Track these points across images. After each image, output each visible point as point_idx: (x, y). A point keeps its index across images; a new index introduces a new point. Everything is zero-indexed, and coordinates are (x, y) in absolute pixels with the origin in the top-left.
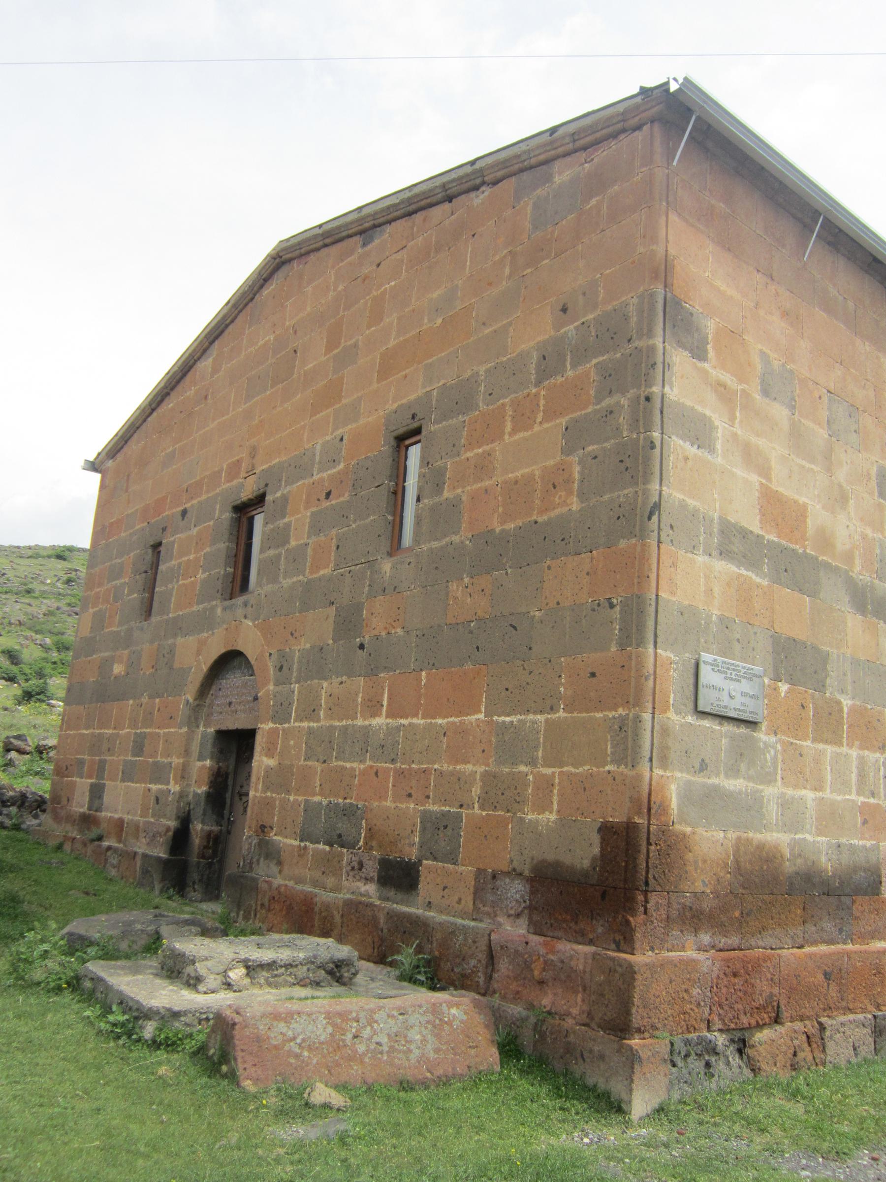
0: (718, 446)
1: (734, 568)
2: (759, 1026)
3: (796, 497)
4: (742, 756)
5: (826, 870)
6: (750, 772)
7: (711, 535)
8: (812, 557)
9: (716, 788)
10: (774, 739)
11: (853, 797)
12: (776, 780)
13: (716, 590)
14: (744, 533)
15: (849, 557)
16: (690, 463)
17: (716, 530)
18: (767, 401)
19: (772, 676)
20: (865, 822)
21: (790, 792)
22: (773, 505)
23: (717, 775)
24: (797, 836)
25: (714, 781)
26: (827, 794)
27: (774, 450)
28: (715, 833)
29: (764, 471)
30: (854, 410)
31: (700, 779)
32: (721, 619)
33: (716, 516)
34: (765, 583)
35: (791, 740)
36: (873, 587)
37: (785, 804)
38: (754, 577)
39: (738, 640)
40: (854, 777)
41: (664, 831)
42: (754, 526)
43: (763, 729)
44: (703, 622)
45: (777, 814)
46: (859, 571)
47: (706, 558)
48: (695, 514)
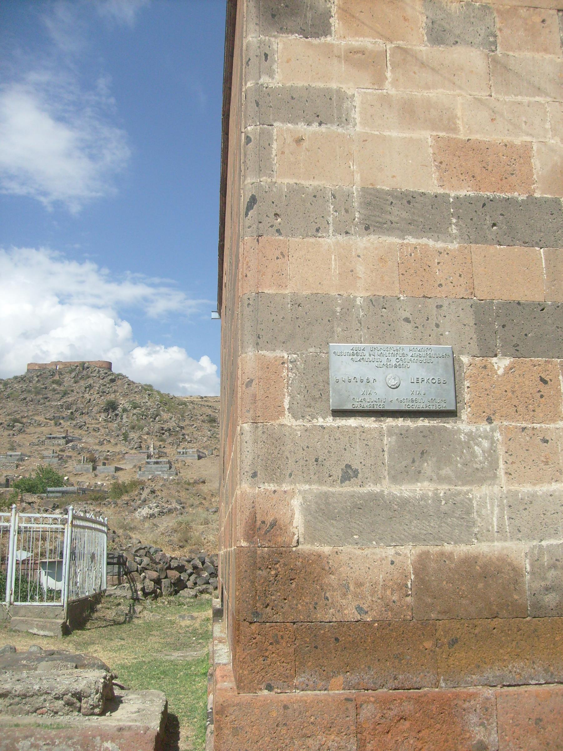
0: (356, 115)
1: (393, 240)
3: (507, 139)
6: (443, 472)
7: (347, 211)
8: (546, 201)
9: (375, 498)
10: (488, 427)
12: (495, 477)
13: (360, 269)
14: (409, 199)
16: (305, 144)
17: (356, 204)
18: (442, 48)
19: (476, 352)
21: (527, 489)
22: (458, 154)
23: (378, 480)
24: (544, 543)
25: (377, 489)
28: (377, 550)
31: (348, 489)
32: (372, 301)
33: (355, 190)
34: (454, 246)
35: (524, 425)
37: (515, 505)
38: (431, 243)
39: (407, 320)
42: (433, 187)
43: (464, 417)
44: (338, 309)
45: (501, 518)
47: (341, 238)
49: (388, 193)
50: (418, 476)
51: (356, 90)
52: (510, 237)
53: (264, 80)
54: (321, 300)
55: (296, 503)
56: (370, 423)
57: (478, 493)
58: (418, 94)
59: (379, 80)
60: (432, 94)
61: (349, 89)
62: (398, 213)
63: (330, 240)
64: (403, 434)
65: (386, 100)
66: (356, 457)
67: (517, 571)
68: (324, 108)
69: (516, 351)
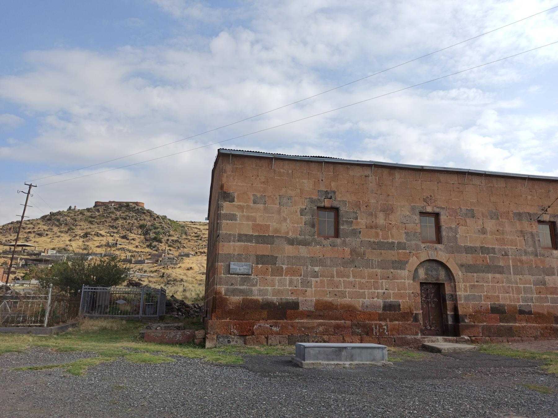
0: (238, 219)
2: (246, 335)
4: (243, 282)
9: (237, 289)
11: (287, 287)
13: (237, 249)
14: (246, 235)
20: (292, 293)
21: (262, 288)
22: (256, 227)
26: (277, 287)
30: (290, 198)
31: (232, 287)
32: (238, 255)
37: (260, 290)
40: (288, 283)
41: (221, 297)
42: (251, 233)
46: (290, 235)
48: (230, 235)
50: (244, 285)
51: (239, 214)
52: (264, 243)
53: (222, 212)
54: (229, 254)
55: (223, 289)
56: (236, 276)
57: (254, 288)
58: (250, 214)
59: (243, 212)
60: (253, 214)
61: (237, 214)
62: (244, 238)
63: (232, 243)
64: (242, 278)
66: (233, 282)
67: (259, 301)
68: (232, 217)
69: (263, 264)
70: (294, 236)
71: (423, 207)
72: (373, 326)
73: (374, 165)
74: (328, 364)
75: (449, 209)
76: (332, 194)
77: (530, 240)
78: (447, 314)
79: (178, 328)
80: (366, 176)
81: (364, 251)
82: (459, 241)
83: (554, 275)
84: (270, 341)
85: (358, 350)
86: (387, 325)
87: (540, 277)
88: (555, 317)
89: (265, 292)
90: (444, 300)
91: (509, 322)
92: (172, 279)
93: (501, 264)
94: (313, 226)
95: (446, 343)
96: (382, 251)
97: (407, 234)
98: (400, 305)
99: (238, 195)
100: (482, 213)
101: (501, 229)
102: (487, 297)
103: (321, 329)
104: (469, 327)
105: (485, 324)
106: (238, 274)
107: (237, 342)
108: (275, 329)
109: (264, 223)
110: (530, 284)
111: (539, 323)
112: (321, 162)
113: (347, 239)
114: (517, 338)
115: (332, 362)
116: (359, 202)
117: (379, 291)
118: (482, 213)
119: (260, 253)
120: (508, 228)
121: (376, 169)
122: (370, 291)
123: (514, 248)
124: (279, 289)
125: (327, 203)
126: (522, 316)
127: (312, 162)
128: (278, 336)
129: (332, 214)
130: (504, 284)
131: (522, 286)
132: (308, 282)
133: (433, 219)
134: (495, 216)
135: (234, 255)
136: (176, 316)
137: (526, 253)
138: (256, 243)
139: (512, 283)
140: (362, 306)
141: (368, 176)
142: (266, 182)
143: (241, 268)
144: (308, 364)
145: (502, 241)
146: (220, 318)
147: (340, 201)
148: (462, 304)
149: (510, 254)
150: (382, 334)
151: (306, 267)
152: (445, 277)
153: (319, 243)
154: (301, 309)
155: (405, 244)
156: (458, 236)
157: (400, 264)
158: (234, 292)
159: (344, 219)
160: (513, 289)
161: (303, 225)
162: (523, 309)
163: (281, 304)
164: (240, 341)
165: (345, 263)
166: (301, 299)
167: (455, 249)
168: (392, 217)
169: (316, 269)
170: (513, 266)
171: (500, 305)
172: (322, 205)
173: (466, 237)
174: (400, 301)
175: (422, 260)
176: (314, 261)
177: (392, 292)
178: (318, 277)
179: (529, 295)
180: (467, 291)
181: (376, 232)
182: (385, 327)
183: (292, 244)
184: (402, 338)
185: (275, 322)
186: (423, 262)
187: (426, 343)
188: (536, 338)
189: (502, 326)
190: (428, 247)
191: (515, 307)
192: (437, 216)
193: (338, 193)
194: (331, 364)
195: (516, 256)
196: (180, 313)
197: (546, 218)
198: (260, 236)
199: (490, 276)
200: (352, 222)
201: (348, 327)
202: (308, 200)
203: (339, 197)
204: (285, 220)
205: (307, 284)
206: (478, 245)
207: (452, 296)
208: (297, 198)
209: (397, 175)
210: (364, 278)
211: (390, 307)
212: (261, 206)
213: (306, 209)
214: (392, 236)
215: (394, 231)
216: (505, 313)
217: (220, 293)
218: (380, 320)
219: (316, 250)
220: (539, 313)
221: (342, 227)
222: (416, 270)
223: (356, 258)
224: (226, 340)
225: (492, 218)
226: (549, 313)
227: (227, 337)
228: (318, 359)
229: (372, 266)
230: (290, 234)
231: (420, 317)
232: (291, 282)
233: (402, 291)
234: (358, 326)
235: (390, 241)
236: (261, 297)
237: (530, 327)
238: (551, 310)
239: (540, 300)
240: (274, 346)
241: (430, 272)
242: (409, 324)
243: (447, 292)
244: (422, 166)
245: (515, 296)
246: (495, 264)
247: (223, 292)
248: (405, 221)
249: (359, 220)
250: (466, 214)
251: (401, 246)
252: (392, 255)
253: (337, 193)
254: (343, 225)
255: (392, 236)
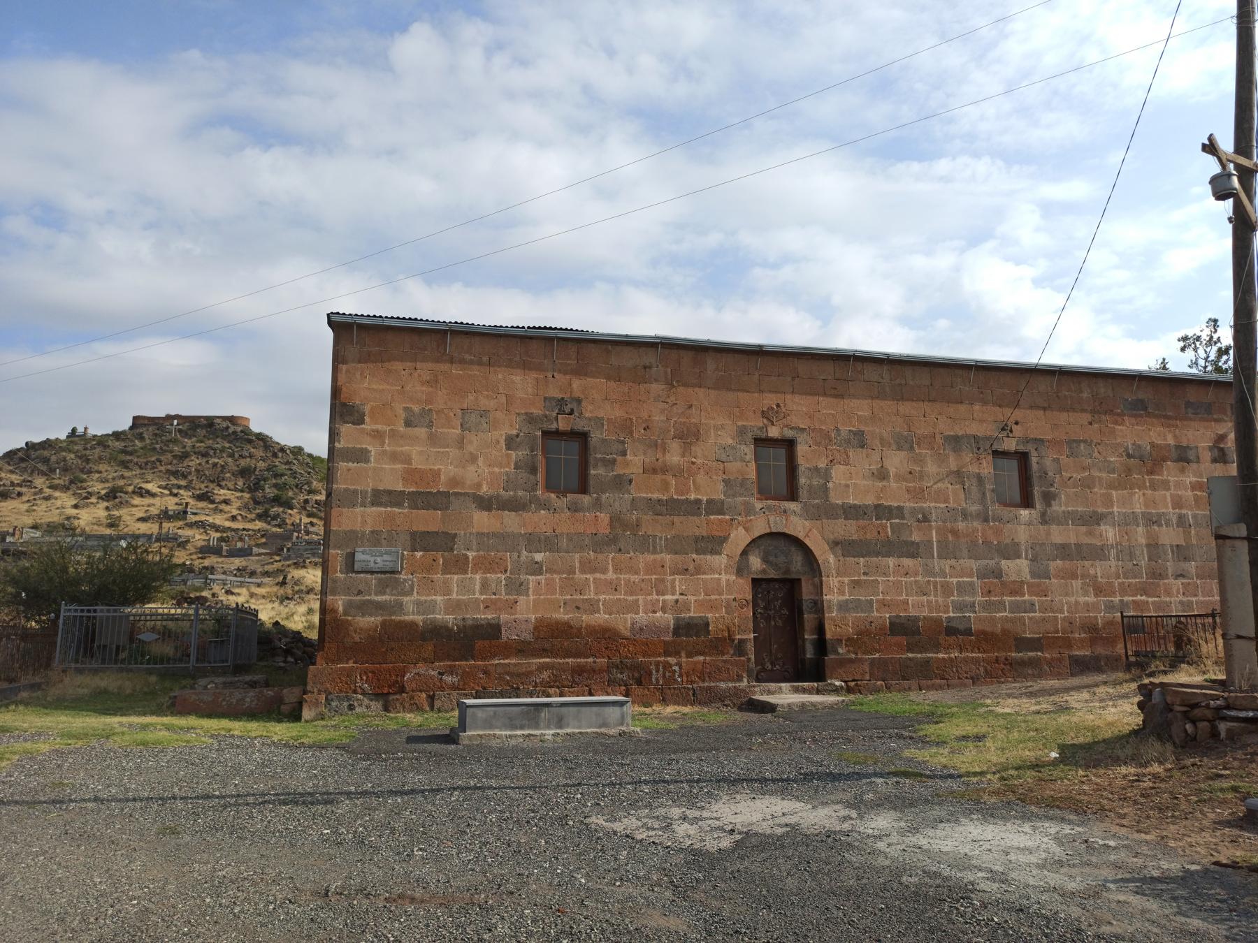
2: (389, 693)
5: (452, 630)
14: (390, 492)
15: (479, 485)
21: (423, 598)
22: (411, 475)
27: (414, 451)
29: (407, 460)
30: (484, 414)
31: (359, 598)
32: (372, 532)
36: (498, 497)
37: (418, 603)
40: (477, 587)
41: (335, 619)
42: (400, 488)
48: (355, 492)
49: (384, 491)
50: (384, 593)
54: (352, 532)
56: (369, 576)
57: (406, 599)
59: (383, 444)
61: (370, 448)
62: (385, 498)
63: (359, 509)
64: (380, 579)
65: (384, 452)
66: (361, 587)
68: (360, 456)
69: (424, 549)
70: (492, 492)
71: (761, 429)
72: (653, 667)
73: (662, 344)
74: (510, 736)
75: (813, 430)
76: (574, 405)
77: (974, 489)
78: (804, 640)
79: (253, 685)
80: (645, 368)
81: (638, 520)
82: (832, 494)
83: (1019, 557)
84: (437, 704)
85: (572, 709)
86: (679, 664)
87: (991, 562)
88: (1016, 639)
89: (432, 607)
90: (801, 613)
91: (926, 651)
92: (303, 588)
93: (915, 537)
94: (533, 470)
95: (796, 695)
96: (676, 519)
97: (727, 482)
98: (708, 624)
99: (372, 410)
100: (882, 439)
101: (917, 469)
102: (884, 604)
103: (545, 675)
104: (843, 663)
105: (877, 655)
106: (372, 572)
107: (368, 707)
108: (448, 679)
109: (428, 467)
110: (971, 576)
111: (985, 652)
112: (549, 340)
113: (604, 497)
114: (938, 681)
115: (519, 732)
116: (631, 419)
117: (666, 597)
118: (882, 439)
119: (420, 527)
120: (931, 468)
121: (667, 352)
122: (649, 598)
123: (943, 505)
124: (459, 600)
125: (563, 424)
126: (951, 639)
127: (531, 338)
128: (455, 693)
129: (575, 446)
130: (919, 578)
131: (955, 580)
132: (521, 584)
133: (782, 452)
134: (905, 443)
135: (364, 534)
136: (282, 664)
137: (965, 515)
138: (410, 507)
139: (934, 575)
140: (632, 628)
141: (650, 367)
142: (433, 382)
143: (379, 560)
144: (470, 738)
145: (918, 494)
146: (333, 662)
147: (590, 419)
148: (832, 619)
149: (934, 517)
150: (669, 681)
151: (515, 555)
152: (802, 565)
153: (545, 506)
154: (504, 638)
155: (723, 502)
156: (830, 485)
157: (713, 544)
158: (365, 608)
159: (599, 456)
160: (935, 587)
161: (511, 469)
162: (953, 624)
163: (463, 629)
164: (376, 706)
165: (602, 544)
166: (504, 617)
167: (824, 511)
168: (697, 449)
169: (539, 557)
170: (938, 542)
171: (908, 618)
172: (553, 427)
173: (847, 486)
174: (710, 615)
175: (757, 534)
176: (534, 541)
177: (692, 599)
178: (541, 574)
179: (967, 598)
180: (843, 593)
181: (664, 480)
182: (677, 668)
183: (489, 509)
184: (709, 688)
185: (450, 666)
186: (760, 537)
187: (758, 697)
188: (975, 680)
189: (910, 659)
190: (769, 508)
191: (938, 621)
192: (789, 445)
193: (579, 403)
194: (516, 736)
195: (945, 521)
196: (290, 659)
197: (1010, 445)
198: (420, 493)
199: (891, 562)
200: (615, 460)
201: (601, 671)
202: (523, 417)
203: (589, 411)
204: (473, 459)
205: (517, 587)
206: (870, 500)
207: (815, 603)
208: (499, 415)
209: (711, 363)
210: (636, 573)
211: (690, 632)
212: (421, 432)
213: (517, 436)
214: (697, 488)
215: (701, 478)
216: (919, 633)
217: (334, 611)
218: (667, 654)
219: (539, 521)
220: (984, 633)
221: (592, 472)
222: (745, 553)
223: (621, 536)
224: (346, 704)
225: (900, 448)
226: (1004, 632)
227: (349, 699)
228: (491, 727)
229: (654, 547)
230: (485, 488)
231: (751, 647)
232: (485, 586)
233: (713, 597)
234: (621, 667)
235: (693, 497)
236: (421, 617)
237: (965, 660)
238: (1008, 626)
239: (988, 606)
240: (446, 712)
241: (771, 558)
242: (725, 661)
243: (805, 597)
244: (760, 346)
245: (940, 600)
246: (904, 538)
247: (341, 609)
248: (724, 457)
249: (629, 457)
250: (848, 442)
251: (714, 507)
252: (695, 526)
253: (584, 403)
254: (596, 467)
255: (697, 488)
